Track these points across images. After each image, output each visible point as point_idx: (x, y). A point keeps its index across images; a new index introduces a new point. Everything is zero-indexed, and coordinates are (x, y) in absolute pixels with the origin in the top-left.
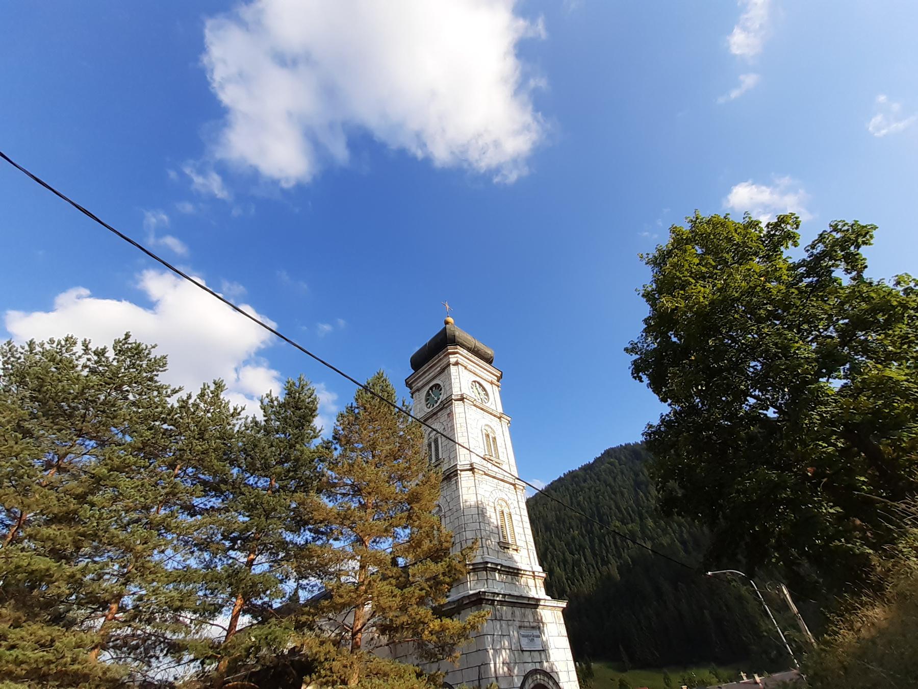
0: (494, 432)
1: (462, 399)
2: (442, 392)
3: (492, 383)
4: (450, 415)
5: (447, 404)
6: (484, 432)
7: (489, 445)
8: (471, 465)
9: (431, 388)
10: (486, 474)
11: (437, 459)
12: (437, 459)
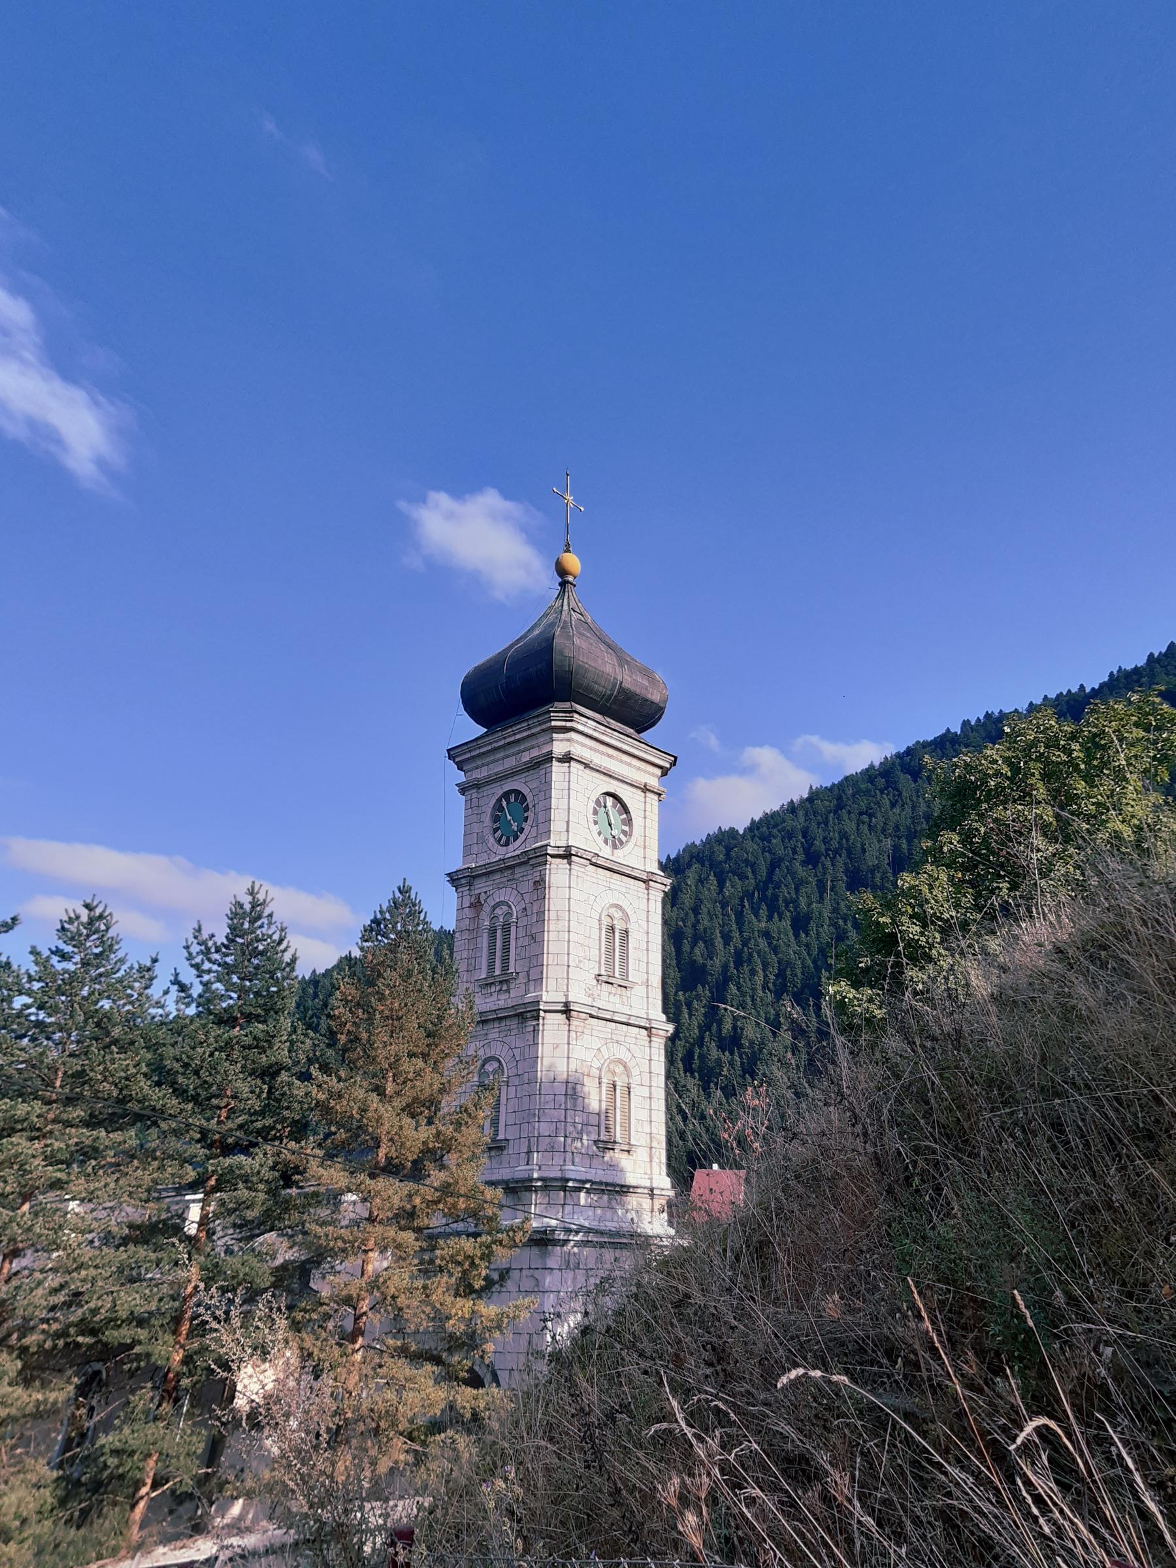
0: (626, 917)
1: (567, 855)
2: (530, 814)
3: (645, 789)
4: (540, 885)
5: (537, 858)
6: (606, 921)
7: (611, 951)
8: (567, 1004)
9: (506, 795)
10: (592, 1016)
11: (505, 967)
12: (505, 967)
